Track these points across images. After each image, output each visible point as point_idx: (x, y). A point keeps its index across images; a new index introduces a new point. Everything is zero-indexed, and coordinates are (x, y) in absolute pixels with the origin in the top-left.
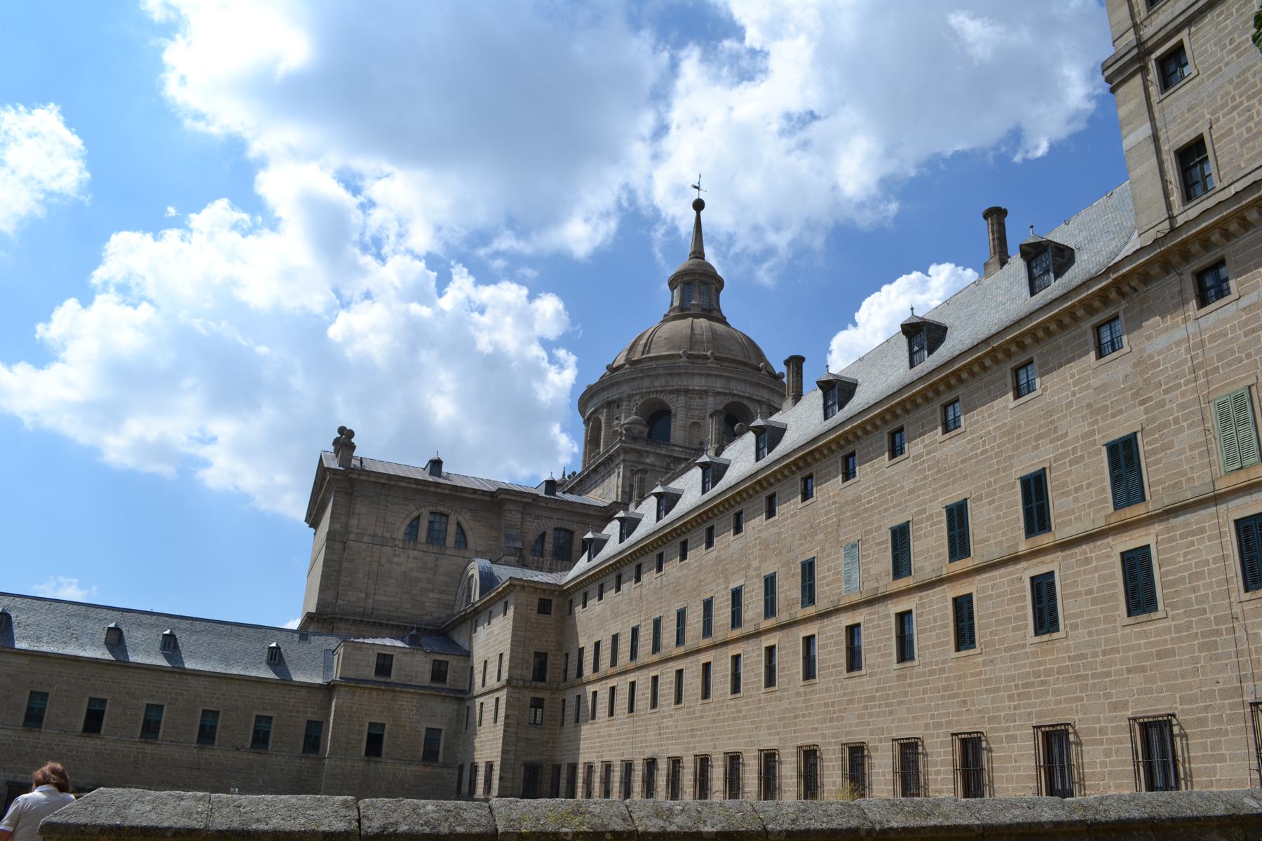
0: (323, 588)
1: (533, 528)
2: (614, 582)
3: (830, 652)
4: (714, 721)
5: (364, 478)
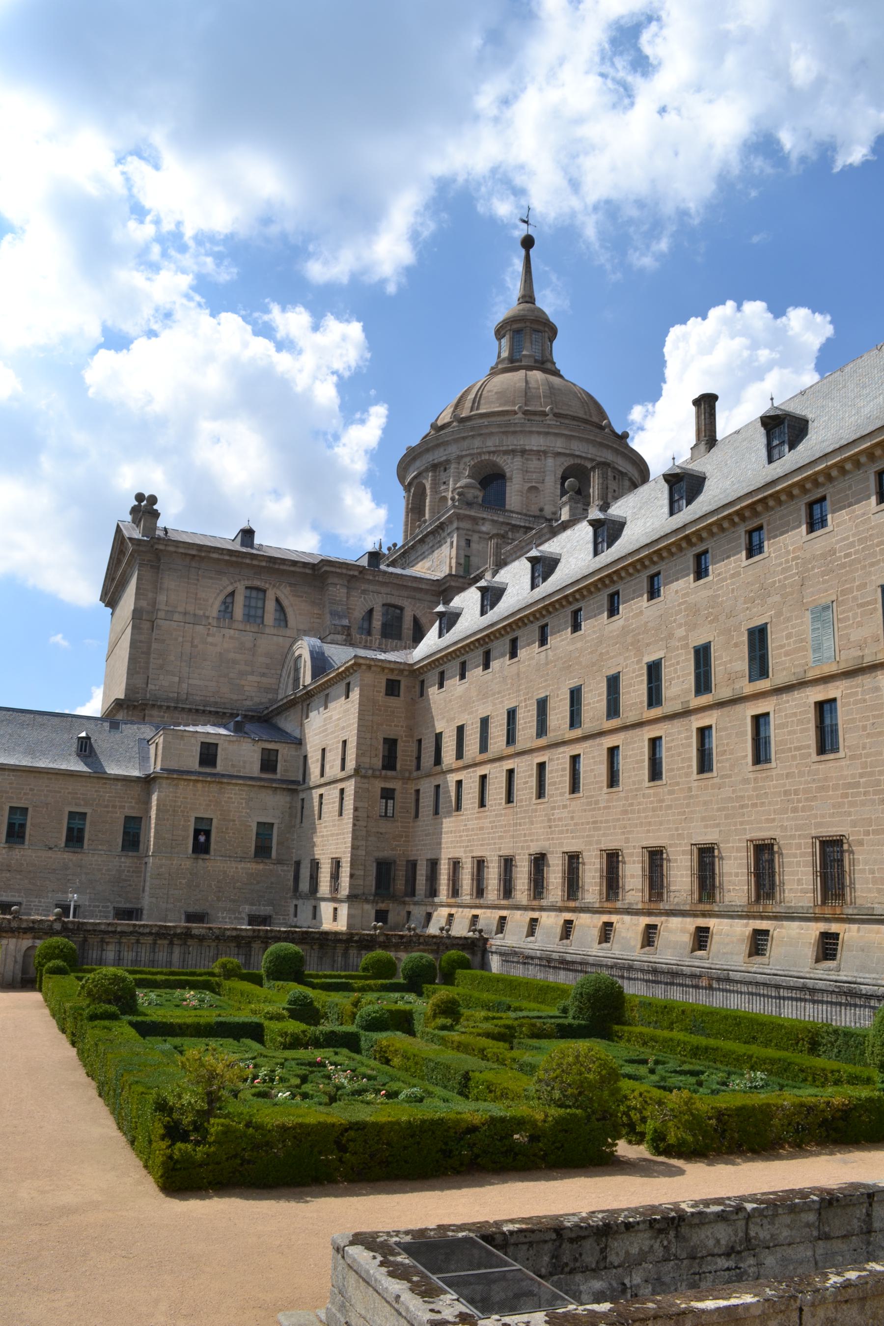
0: (132, 671)
1: (359, 605)
2: (480, 660)
3: (794, 732)
4: (625, 812)
5: (172, 549)
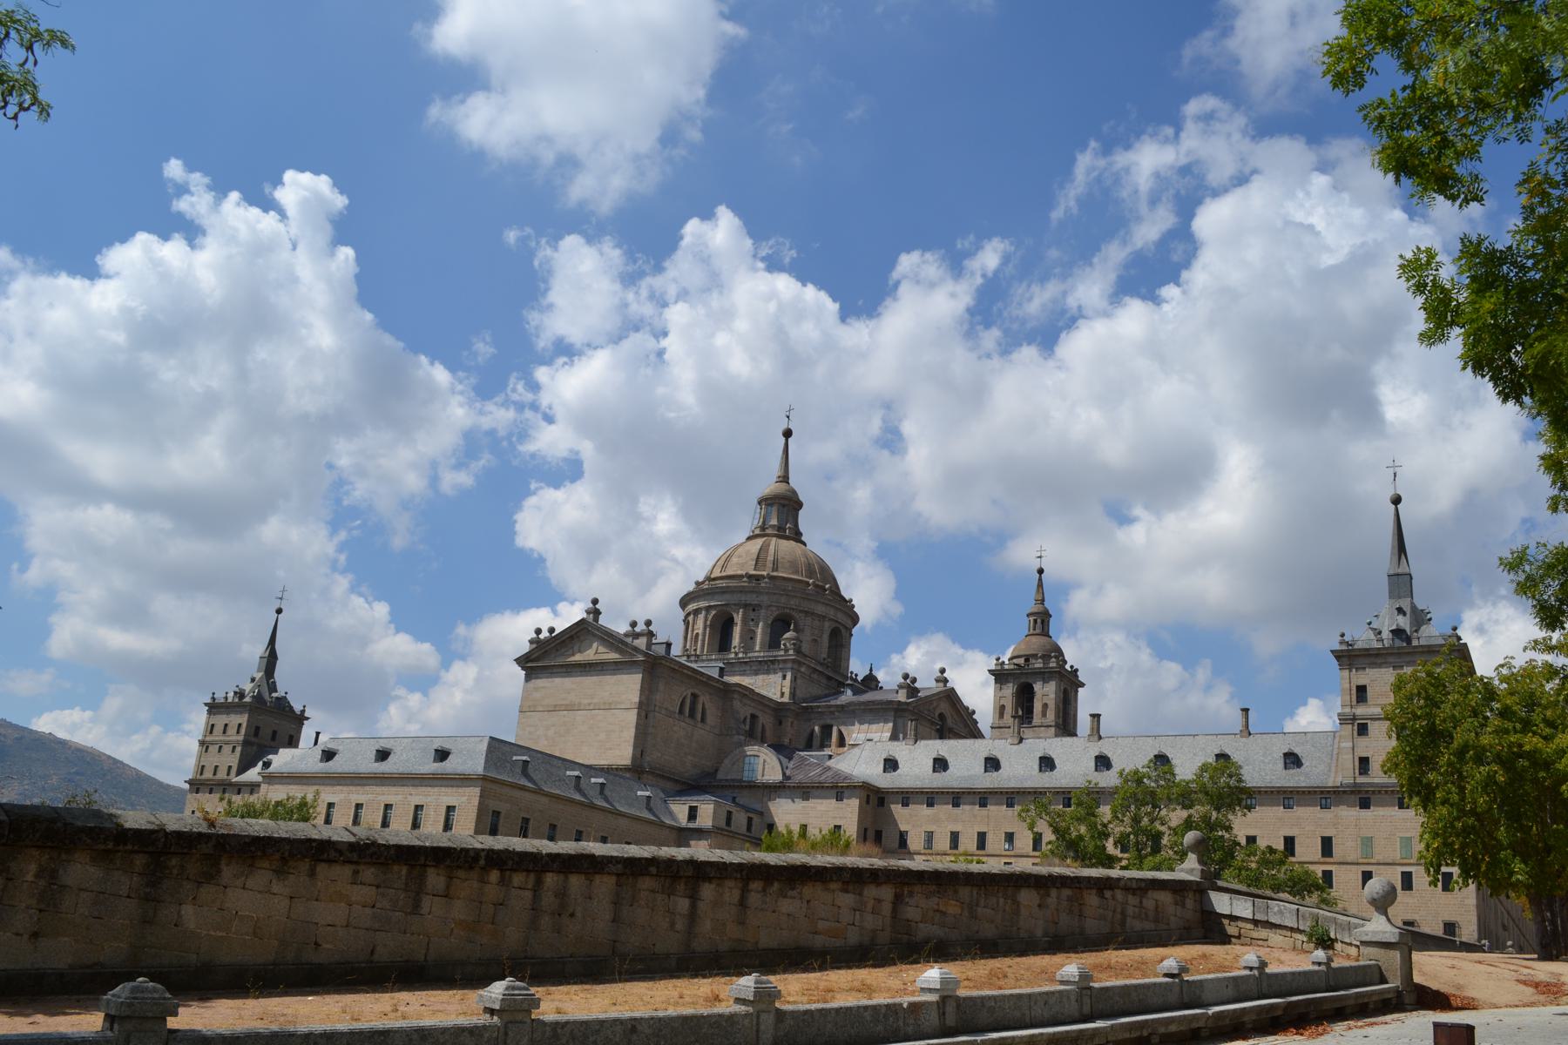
0: (635, 747)
